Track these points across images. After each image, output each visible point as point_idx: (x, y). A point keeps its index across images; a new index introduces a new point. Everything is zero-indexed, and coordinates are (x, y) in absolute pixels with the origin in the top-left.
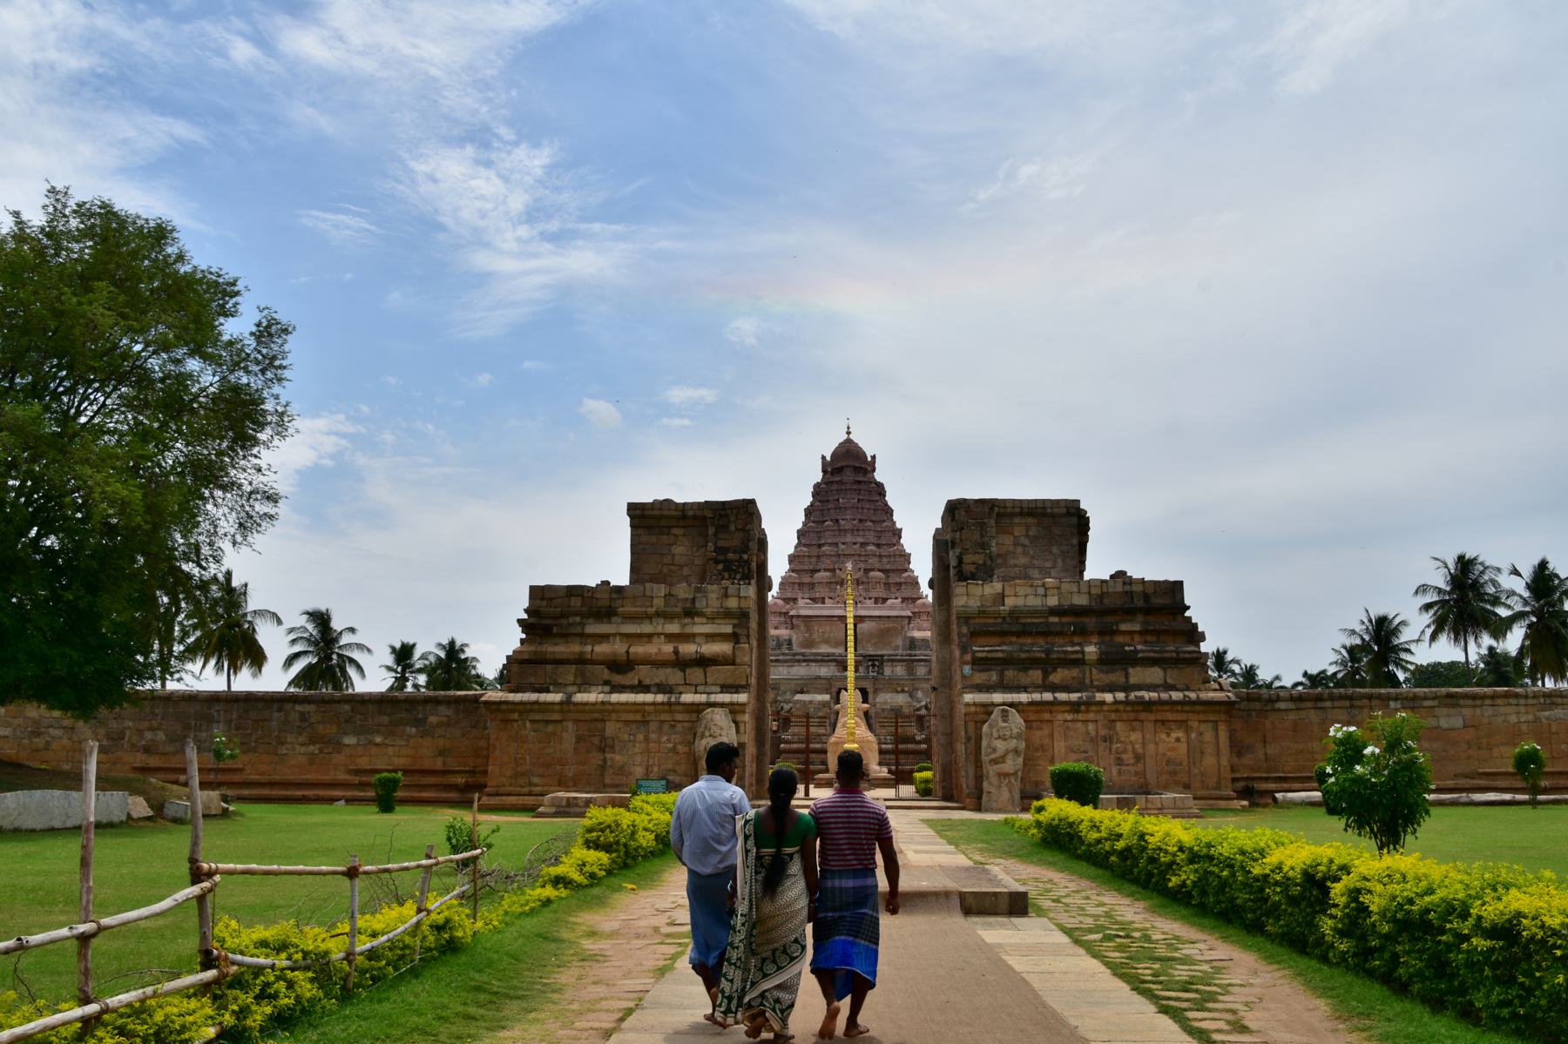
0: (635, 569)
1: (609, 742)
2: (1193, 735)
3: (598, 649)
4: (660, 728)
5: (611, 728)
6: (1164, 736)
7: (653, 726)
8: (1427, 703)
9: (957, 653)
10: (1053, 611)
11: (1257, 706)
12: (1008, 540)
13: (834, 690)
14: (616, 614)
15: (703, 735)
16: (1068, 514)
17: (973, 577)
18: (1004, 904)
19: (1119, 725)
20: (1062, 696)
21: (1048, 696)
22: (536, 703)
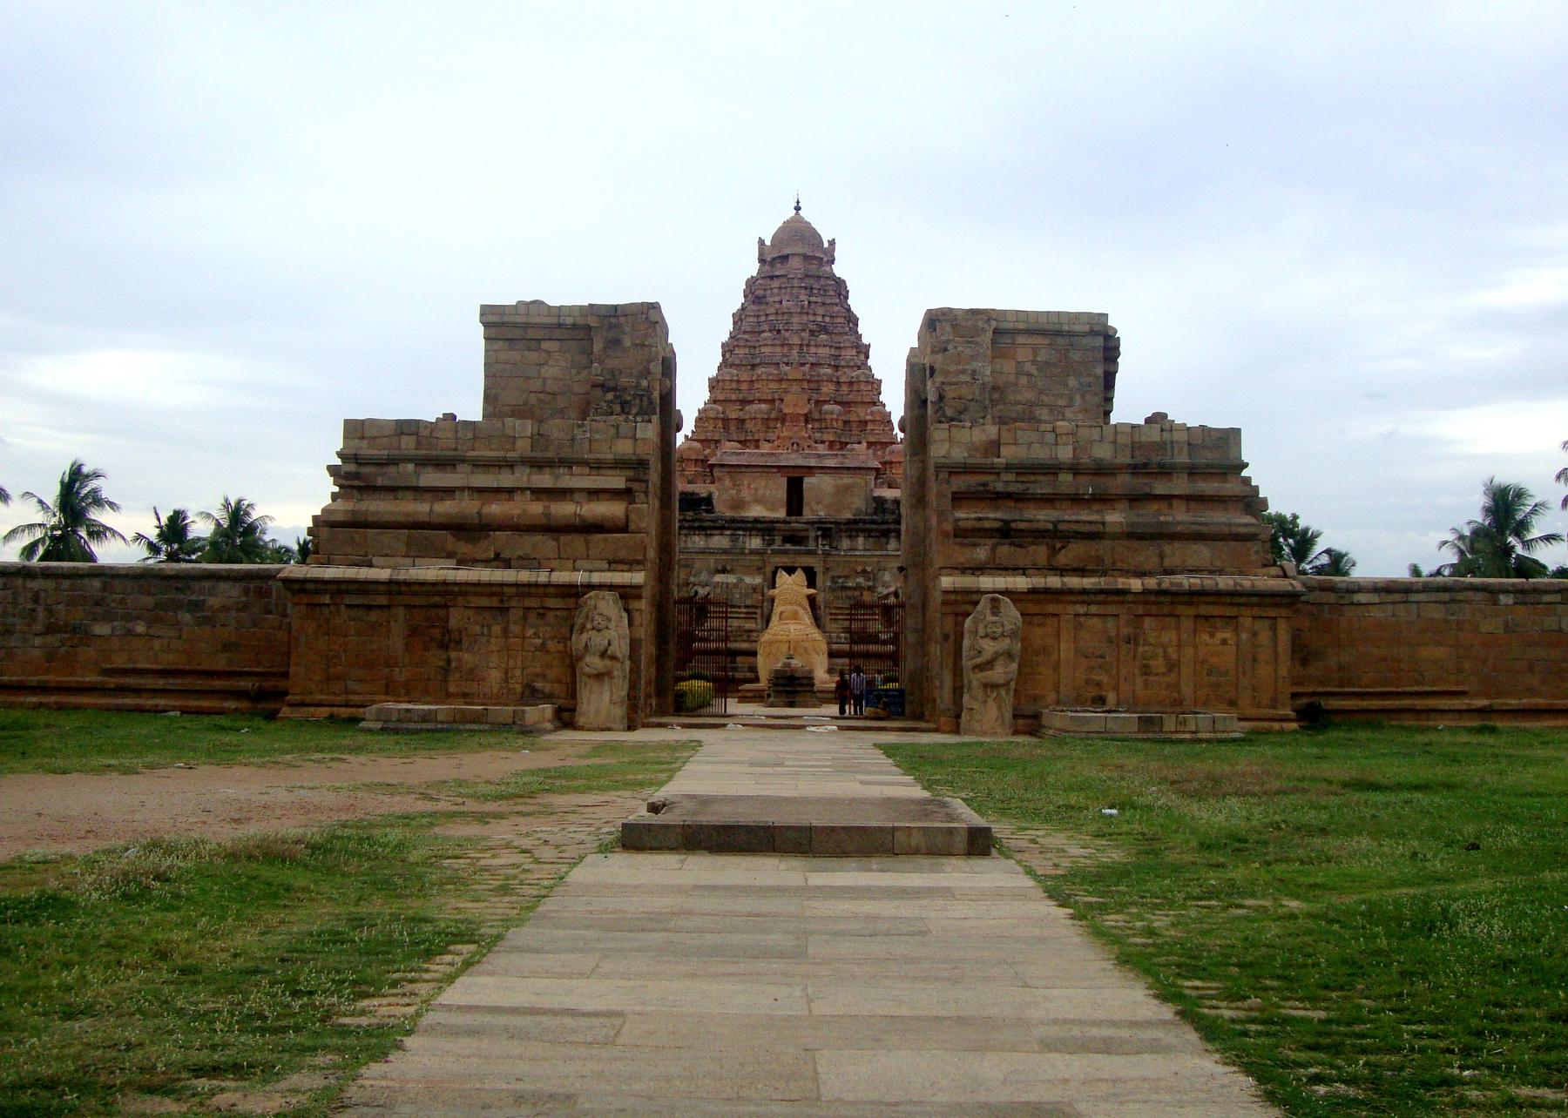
0: (489, 398)
1: (455, 636)
2: (1244, 636)
4: (525, 618)
5: (456, 618)
6: (1206, 637)
7: (515, 615)
8: (1547, 598)
12: (1009, 367)
13: (769, 569)
14: (463, 461)
15: (582, 629)
18: (961, 842)
19: (1147, 622)
20: (1074, 582)
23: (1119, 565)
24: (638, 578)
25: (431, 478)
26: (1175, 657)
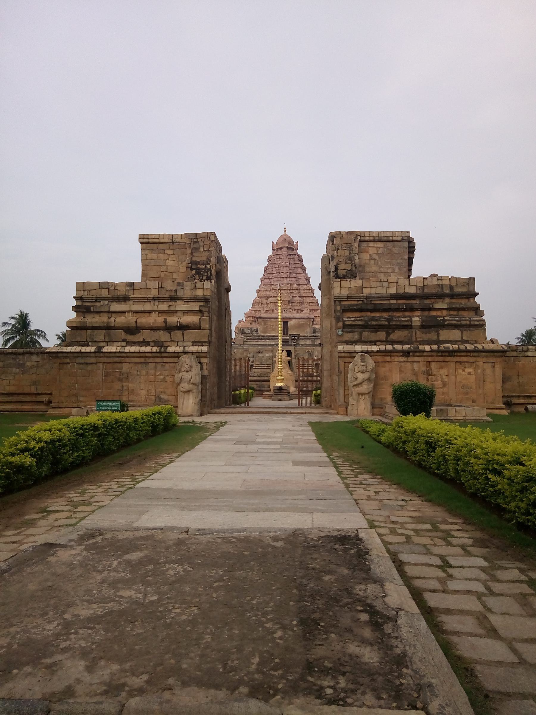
0: (144, 275)
1: (125, 376)
4: (155, 367)
6: (461, 371)
7: (151, 366)
11: (515, 354)
12: (365, 256)
15: (179, 372)
16: (403, 240)
20: (398, 347)
21: (389, 347)
23: (419, 340)
24: (205, 349)
26: (446, 380)
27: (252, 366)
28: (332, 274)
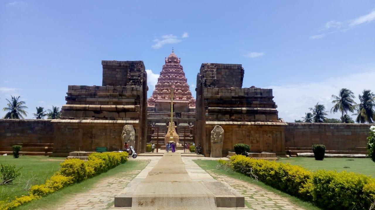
3: (91, 106)
5: (94, 131)
6: (265, 135)
9: (204, 109)
10: (233, 97)
12: (220, 76)
13: (167, 122)
15: (124, 133)
17: (210, 86)
20: (235, 123)
21: (231, 123)
22: (69, 123)
25: (89, 99)
26: (258, 140)
27: (153, 130)
28: (203, 85)
